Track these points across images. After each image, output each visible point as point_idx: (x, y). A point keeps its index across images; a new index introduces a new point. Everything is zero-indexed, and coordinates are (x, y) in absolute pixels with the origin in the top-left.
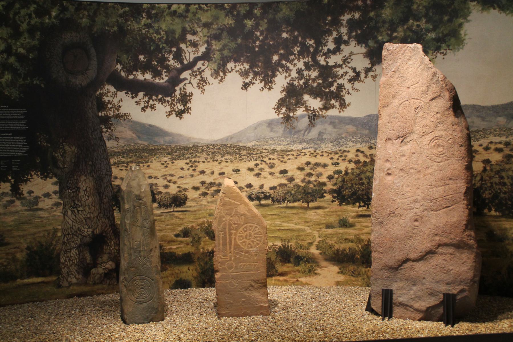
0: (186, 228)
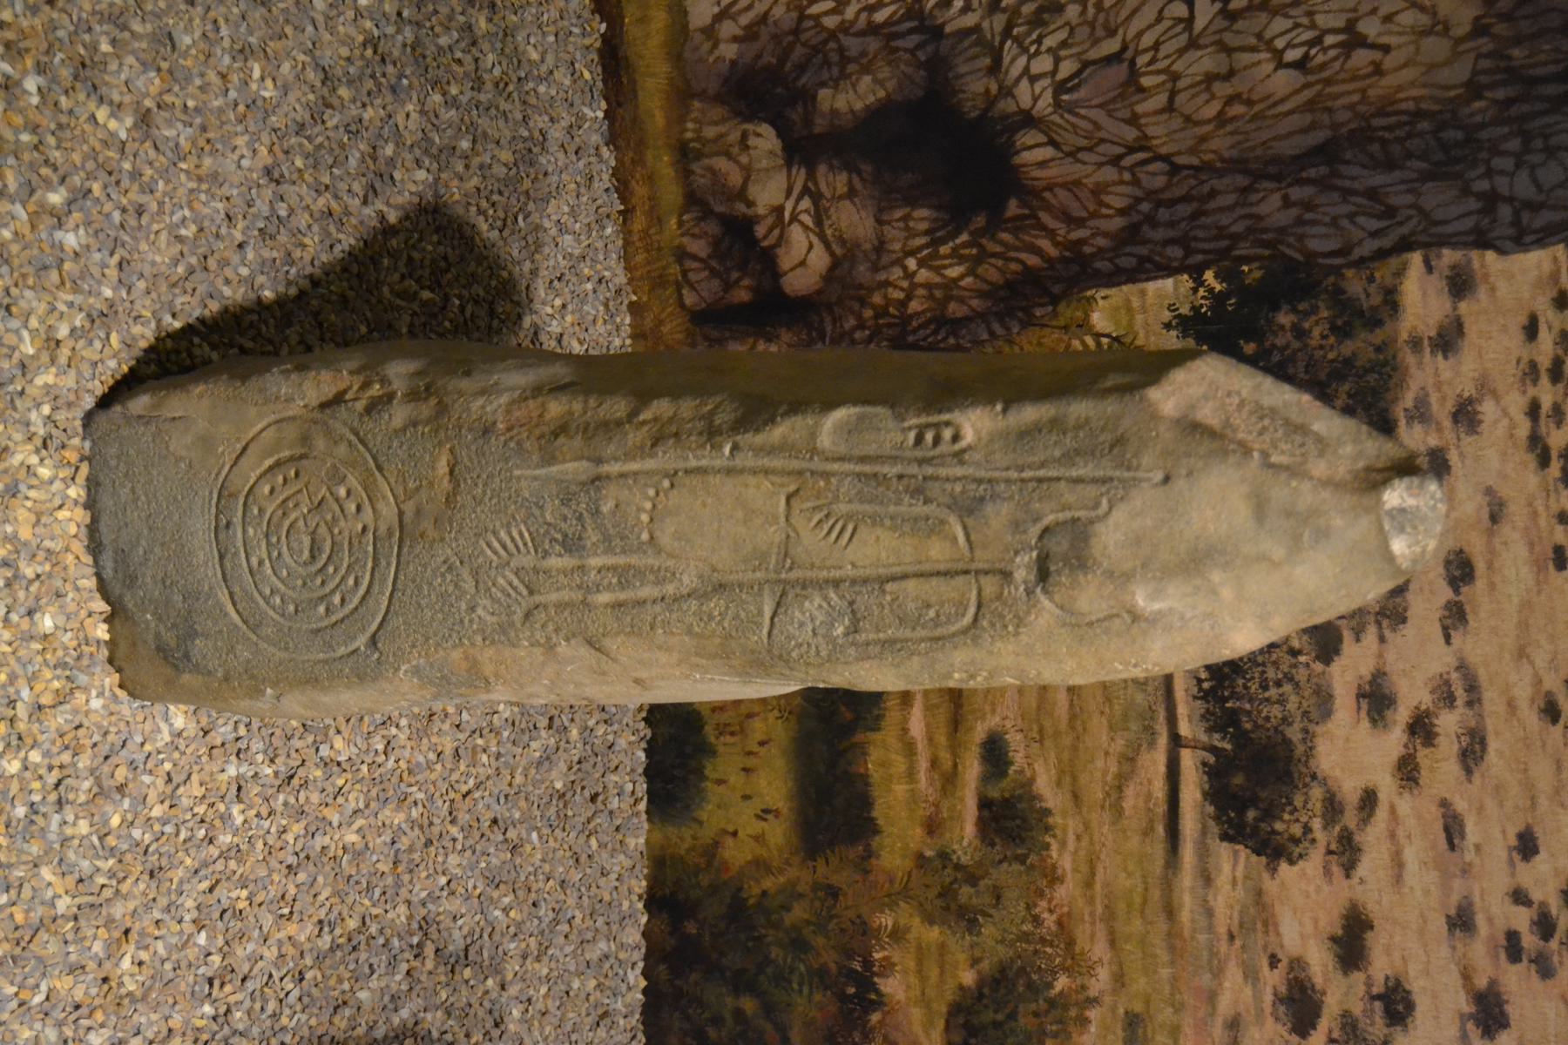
0: (1048, 829)
